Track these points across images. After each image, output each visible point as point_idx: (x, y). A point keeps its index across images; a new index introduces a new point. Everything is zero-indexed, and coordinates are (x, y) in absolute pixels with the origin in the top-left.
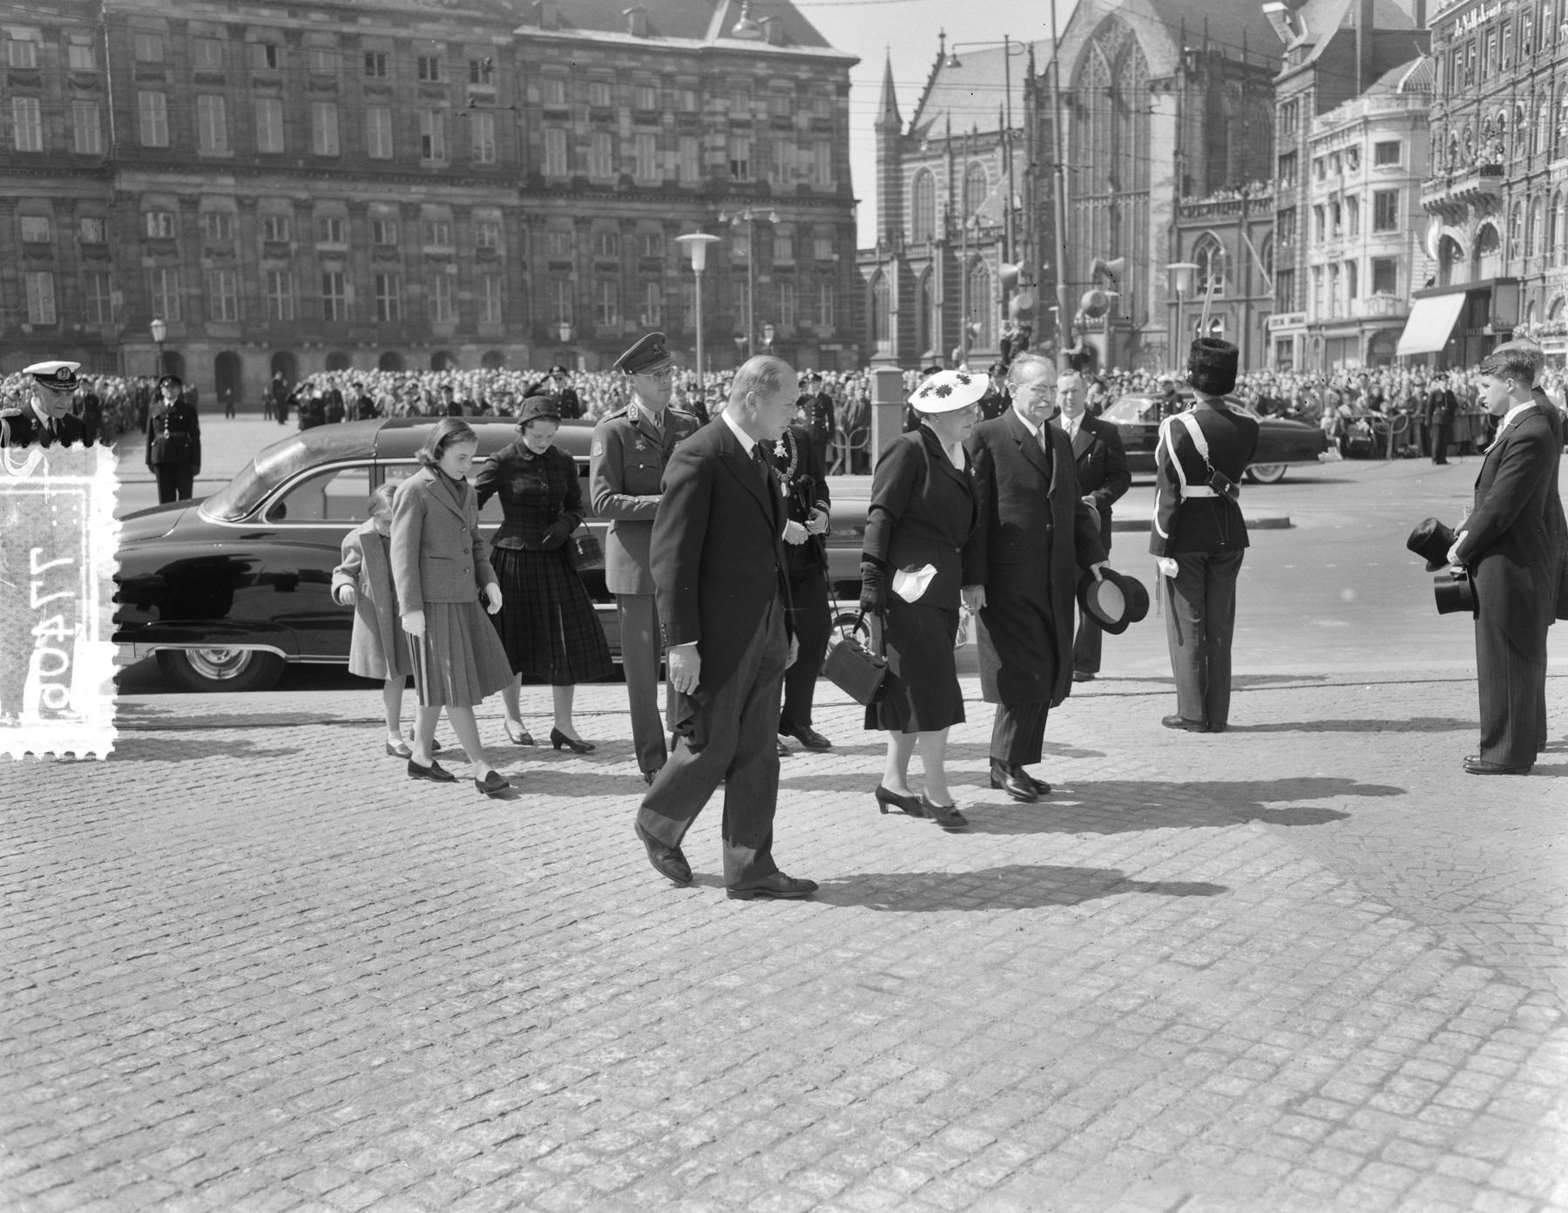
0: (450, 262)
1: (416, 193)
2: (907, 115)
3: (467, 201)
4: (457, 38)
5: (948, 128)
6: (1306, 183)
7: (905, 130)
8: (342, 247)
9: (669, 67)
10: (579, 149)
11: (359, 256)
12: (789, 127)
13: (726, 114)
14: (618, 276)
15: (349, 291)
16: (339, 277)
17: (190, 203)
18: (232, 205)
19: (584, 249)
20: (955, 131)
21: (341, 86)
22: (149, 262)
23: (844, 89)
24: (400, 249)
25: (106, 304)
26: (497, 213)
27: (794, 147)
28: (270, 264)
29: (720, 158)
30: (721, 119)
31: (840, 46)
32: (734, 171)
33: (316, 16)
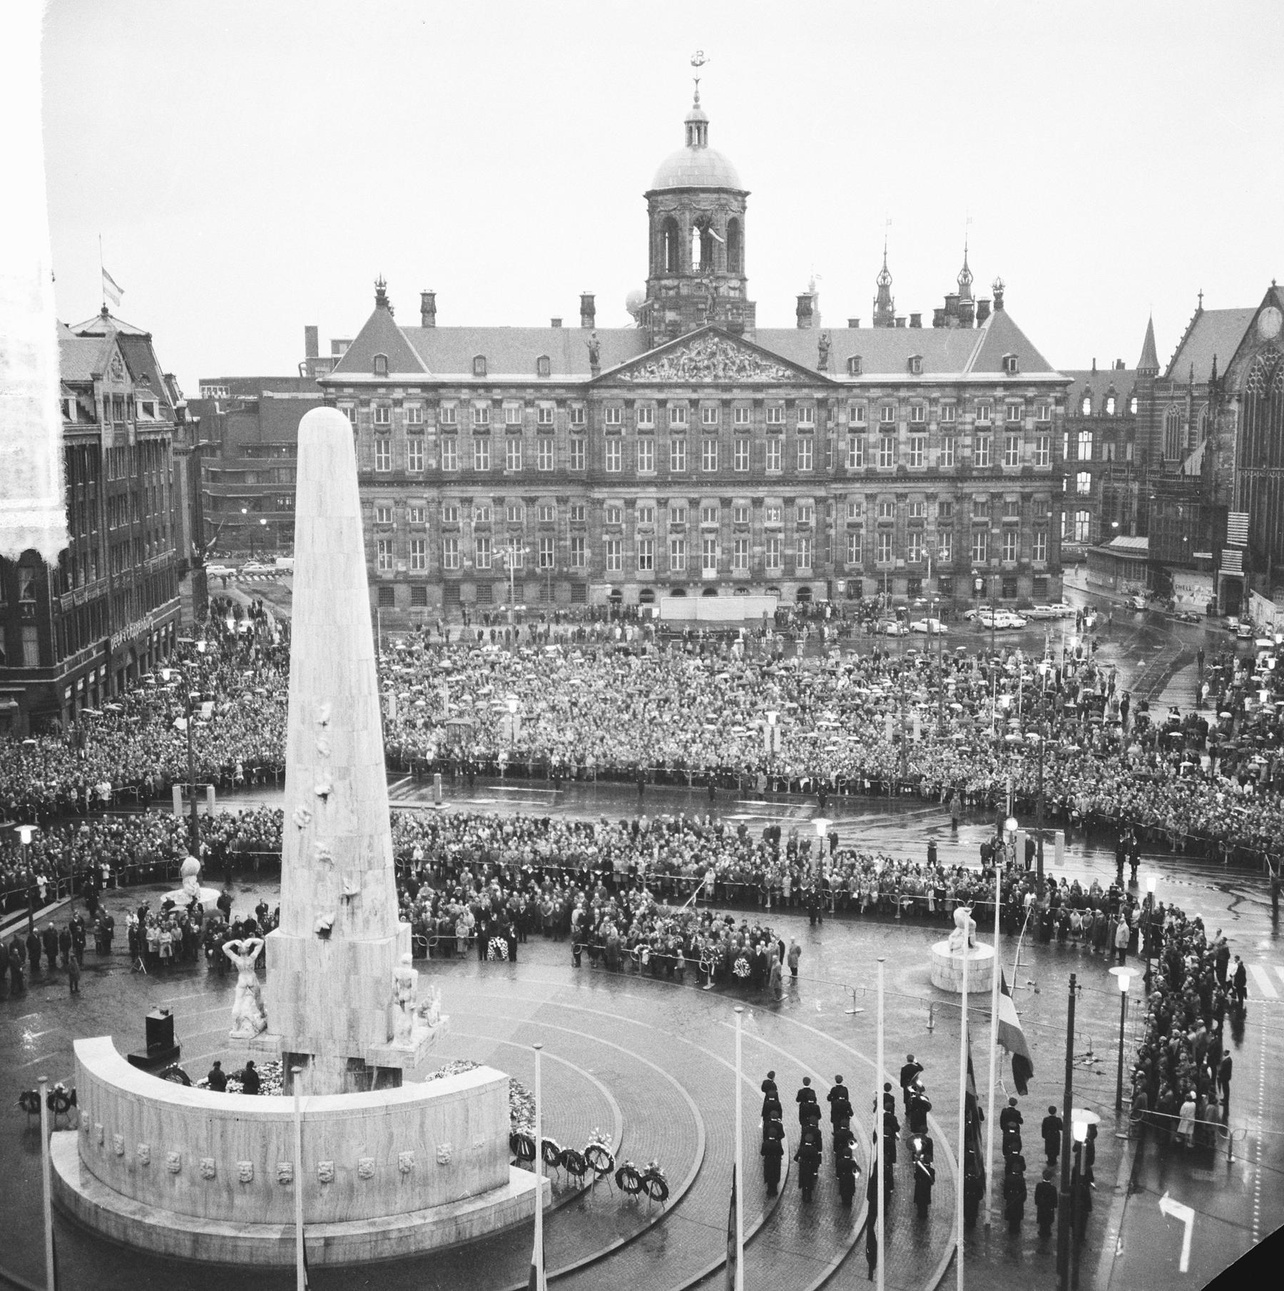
1: (761, 492)
2: (1164, 360)
3: (792, 495)
5: (1192, 376)
7: (1162, 372)
8: (716, 525)
9: (935, 394)
10: (871, 451)
12: (1019, 429)
13: (973, 423)
14: (893, 530)
15: (718, 550)
16: (713, 542)
17: (630, 503)
18: (653, 503)
19: (870, 515)
22: (606, 538)
25: (582, 556)
26: (811, 501)
28: (674, 536)
29: (967, 452)
30: (968, 427)
33: (707, 391)
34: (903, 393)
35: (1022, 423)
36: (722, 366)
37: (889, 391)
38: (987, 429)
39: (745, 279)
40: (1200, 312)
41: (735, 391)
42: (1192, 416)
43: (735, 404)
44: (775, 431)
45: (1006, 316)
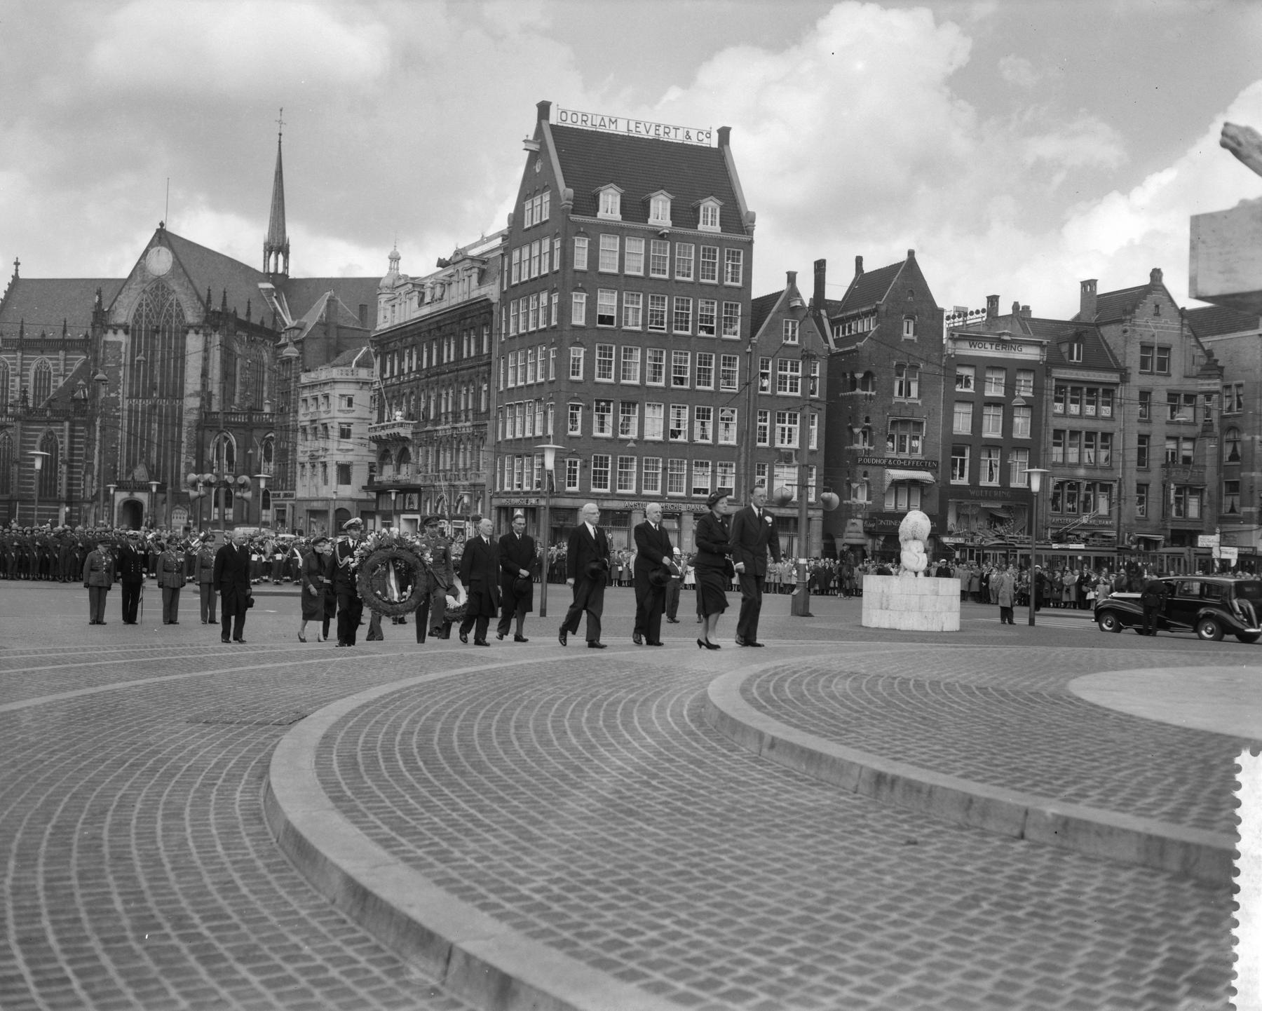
6: (296, 412)
20: (26, 335)
40: (16, 278)
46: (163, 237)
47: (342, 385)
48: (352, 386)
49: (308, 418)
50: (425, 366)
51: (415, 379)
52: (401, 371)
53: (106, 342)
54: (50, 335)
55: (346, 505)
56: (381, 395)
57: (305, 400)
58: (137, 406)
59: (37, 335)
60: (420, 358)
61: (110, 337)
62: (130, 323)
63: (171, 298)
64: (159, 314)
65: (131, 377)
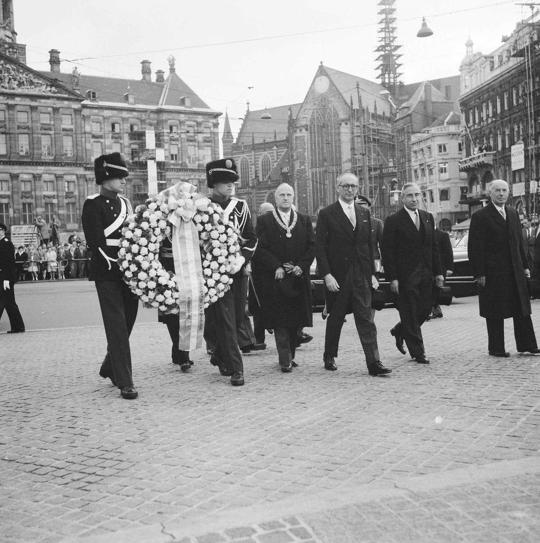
0: (54, 198)
1: (40, 170)
2: (235, 136)
3: (61, 173)
4: (58, 106)
5: (253, 141)
6: (410, 161)
11: (15, 196)
12: (195, 141)
15: (11, 211)
16: (7, 205)
20: (256, 142)
21: (7, 126)
23: (216, 125)
24: (33, 193)
27: (197, 148)
31: (214, 108)
32: (172, 159)
34: (125, 114)
35: (196, 137)
36: (7, 80)
37: (115, 112)
38: (177, 140)
39: (16, 34)
40: (248, 112)
41: (18, 99)
42: (255, 161)
43: (18, 108)
44: (46, 128)
45: (177, 77)
46: (322, 71)
47: (439, 138)
48: (445, 138)
49: (418, 163)
50: (499, 111)
51: (492, 122)
52: (481, 119)
53: (296, 137)
54: (268, 140)
55: (448, 217)
56: (467, 138)
57: (415, 152)
58: (316, 172)
59: (261, 141)
60: (495, 107)
61: (298, 134)
62: (308, 123)
63: (330, 105)
64: (324, 116)
65: (312, 155)
